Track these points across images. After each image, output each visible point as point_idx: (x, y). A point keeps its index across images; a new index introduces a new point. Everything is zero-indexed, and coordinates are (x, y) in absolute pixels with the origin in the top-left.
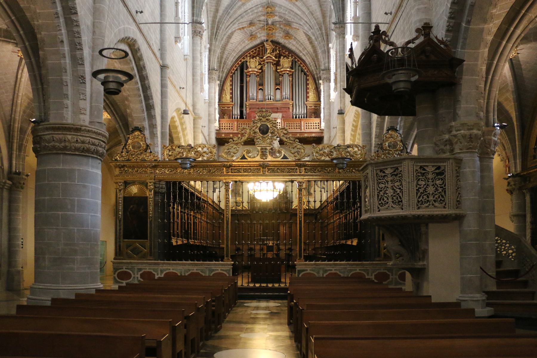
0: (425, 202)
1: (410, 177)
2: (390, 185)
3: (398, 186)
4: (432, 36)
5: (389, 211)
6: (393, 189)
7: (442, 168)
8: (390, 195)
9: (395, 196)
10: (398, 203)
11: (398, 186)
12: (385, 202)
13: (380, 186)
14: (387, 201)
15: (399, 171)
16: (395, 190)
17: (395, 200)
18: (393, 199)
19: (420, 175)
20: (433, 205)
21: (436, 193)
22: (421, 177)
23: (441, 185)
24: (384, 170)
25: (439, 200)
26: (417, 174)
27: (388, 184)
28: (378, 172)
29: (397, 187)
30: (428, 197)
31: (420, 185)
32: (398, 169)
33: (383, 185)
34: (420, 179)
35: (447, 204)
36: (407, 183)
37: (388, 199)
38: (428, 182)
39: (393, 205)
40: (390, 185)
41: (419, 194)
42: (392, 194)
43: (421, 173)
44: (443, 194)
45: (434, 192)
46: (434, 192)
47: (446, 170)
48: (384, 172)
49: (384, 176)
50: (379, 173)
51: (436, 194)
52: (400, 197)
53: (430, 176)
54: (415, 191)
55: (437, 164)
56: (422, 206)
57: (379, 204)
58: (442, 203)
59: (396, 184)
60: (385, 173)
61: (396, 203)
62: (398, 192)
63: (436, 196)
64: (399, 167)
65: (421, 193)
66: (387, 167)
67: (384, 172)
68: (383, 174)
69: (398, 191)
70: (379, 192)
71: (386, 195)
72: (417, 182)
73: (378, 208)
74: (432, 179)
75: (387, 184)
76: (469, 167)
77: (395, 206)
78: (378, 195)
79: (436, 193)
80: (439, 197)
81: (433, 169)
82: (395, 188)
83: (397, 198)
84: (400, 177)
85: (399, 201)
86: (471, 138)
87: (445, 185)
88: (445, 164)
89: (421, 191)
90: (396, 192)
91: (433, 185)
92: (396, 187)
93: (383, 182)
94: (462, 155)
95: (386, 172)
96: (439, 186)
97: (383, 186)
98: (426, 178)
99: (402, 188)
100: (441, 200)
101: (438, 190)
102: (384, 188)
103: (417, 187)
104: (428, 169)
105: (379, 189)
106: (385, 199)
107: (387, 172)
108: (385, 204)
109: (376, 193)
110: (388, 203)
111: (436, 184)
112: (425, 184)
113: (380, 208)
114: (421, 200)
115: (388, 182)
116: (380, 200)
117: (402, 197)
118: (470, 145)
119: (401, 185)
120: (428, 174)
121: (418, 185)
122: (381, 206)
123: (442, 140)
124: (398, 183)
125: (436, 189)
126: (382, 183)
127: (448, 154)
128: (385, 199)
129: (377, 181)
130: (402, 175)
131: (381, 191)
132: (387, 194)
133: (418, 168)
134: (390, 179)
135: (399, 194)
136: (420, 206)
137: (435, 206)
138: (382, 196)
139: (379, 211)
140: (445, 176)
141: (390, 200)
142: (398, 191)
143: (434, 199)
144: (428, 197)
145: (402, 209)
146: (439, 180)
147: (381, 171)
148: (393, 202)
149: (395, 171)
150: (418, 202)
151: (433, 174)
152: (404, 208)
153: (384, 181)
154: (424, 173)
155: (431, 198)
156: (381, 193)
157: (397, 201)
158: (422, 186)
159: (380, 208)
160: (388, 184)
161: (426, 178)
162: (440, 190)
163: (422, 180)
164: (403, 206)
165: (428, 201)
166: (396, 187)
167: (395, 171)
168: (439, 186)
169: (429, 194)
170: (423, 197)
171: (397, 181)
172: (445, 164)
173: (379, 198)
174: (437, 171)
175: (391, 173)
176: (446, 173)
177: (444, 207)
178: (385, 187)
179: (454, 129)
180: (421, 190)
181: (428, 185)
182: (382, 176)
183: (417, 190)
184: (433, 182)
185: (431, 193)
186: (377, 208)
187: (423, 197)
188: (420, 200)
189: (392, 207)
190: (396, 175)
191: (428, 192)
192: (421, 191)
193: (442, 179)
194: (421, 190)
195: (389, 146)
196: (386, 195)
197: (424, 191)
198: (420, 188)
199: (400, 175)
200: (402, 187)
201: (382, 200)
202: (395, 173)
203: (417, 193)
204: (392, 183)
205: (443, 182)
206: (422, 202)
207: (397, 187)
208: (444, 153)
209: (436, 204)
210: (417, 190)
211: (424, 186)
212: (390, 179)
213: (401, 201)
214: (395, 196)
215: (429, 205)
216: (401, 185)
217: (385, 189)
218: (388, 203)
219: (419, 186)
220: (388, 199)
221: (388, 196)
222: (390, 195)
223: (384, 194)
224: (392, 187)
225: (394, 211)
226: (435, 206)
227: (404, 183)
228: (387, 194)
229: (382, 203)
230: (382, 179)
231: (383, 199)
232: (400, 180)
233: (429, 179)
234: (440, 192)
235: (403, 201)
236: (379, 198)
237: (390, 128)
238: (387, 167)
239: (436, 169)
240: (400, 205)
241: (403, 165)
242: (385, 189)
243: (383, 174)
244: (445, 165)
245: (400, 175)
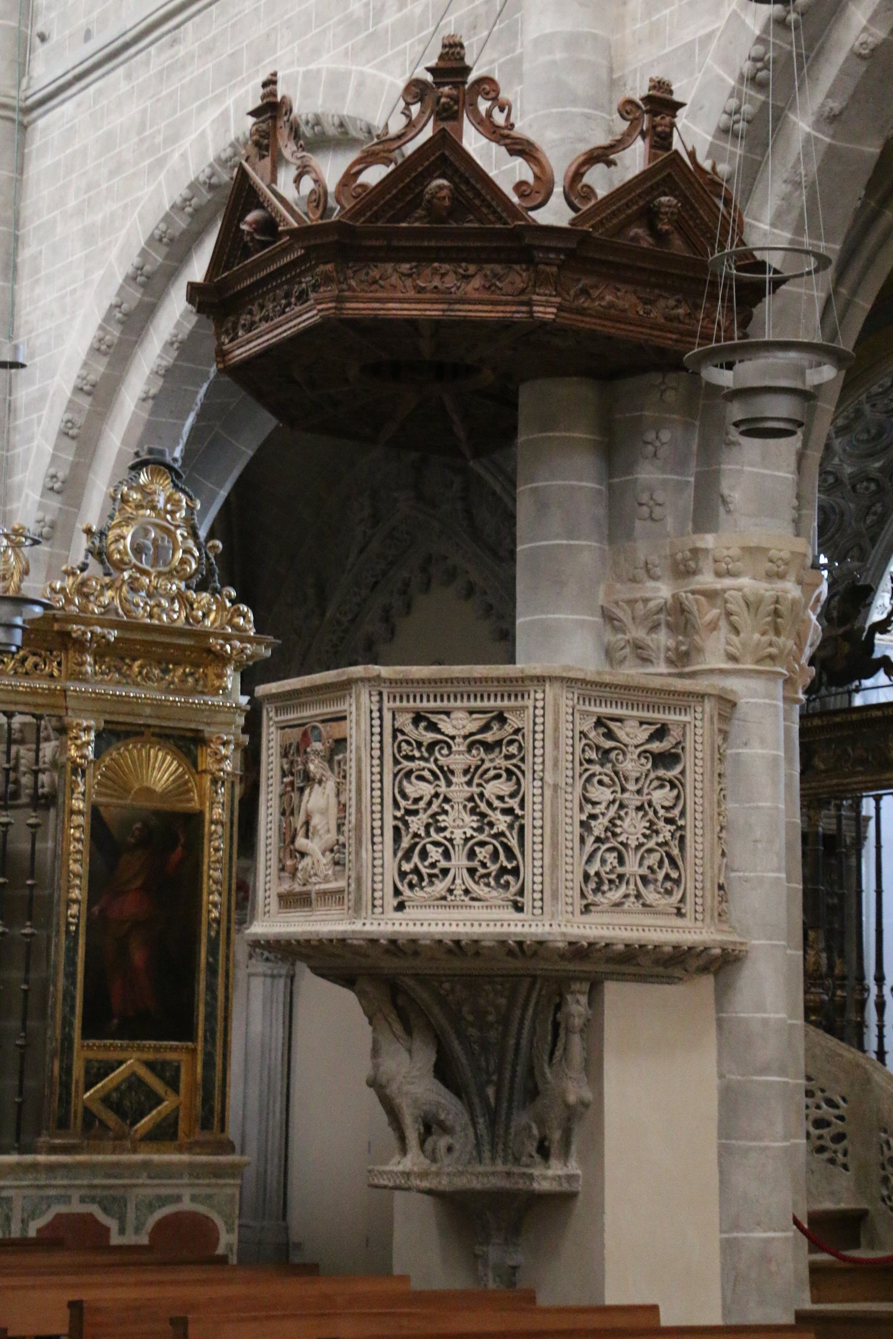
0: (611, 881)
1: (563, 764)
2: (459, 790)
3: (501, 798)
4: (676, 145)
5: (456, 914)
6: (473, 811)
7: (675, 735)
8: (458, 836)
9: (482, 844)
10: (497, 878)
11: (501, 798)
12: (433, 865)
13: (409, 789)
14: (443, 864)
15: (509, 729)
16: (483, 815)
17: (484, 865)
18: (472, 855)
19: (594, 756)
20: (638, 896)
21: (651, 844)
22: (596, 768)
23: (667, 809)
24: (434, 718)
25: (661, 875)
26: (583, 751)
27: (449, 783)
28: (405, 721)
29: (497, 803)
30: (621, 860)
31: (594, 804)
32: (501, 718)
33: (423, 785)
34: (593, 775)
35: (689, 899)
36: (548, 793)
37: (447, 855)
38: (624, 790)
40: (459, 790)
41: (589, 846)
42: (470, 832)
43: (598, 748)
44: (675, 852)
45: (642, 840)
46: (642, 840)
47: (689, 745)
48: (433, 727)
49: (431, 747)
50: (409, 728)
51: (650, 851)
52: (508, 850)
53: (631, 765)
54: (578, 830)
55: (656, 715)
56: (599, 898)
57: (403, 875)
58: (669, 892)
59: (492, 789)
60: (438, 731)
61: (488, 875)
62: (502, 827)
63: (652, 860)
64: (512, 709)
65: (598, 840)
66: (452, 704)
67: (433, 727)
68: (430, 737)
69: (502, 822)
70: (402, 819)
71: (436, 837)
72: (585, 788)
73: (397, 892)
74: (637, 780)
75: (442, 782)
76: (763, 742)
77: (479, 890)
78: (396, 829)
79: (651, 844)
80: (661, 863)
81: (643, 734)
82: (483, 807)
83: (495, 856)
84: (508, 757)
85: (503, 871)
86: (776, 613)
87: (683, 814)
88: (687, 718)
89: (596, 832)
90: (491, 825)
91: (639, 808)
92: (489, 804)
93: (426, 774)
94: (734, 684)
95: (441, 725)
96: (662, 812)
97: (426, 790)
98: (616, 773)
99: (518, 811)
100: (667, 877)
101: (657, 832)
102: (430, 803)
103: (582, 809)
104: (621, 734)
105: (403, 803)
106: (435, 854)
107: (446, 726)
108: (431, 876)
109: (389, 823)
110: (445, 872)
111: (650, 804)
112: (613, 802)
113: (406, 892)
114: (597, 874)
115: (447, 773)
116: (408, 856)
117: (517, 851)
118: (771, 645)
119: (512, 795)
120: (624, 754)
121: (588, 800)
122: (411, 886)
123: (640, 605)
124: (503, 787)
125: (652, 823)
126: (421, 778)
127: (663, 668)
128: (435, 854)
129: (396, 762)
130: (520, 748)
131: (415, 813)
133: (587, 725)
134: (458, 760)
135: (502, 834)
136: (591, 898)
137: (644, 905)
138: (416, 835)
139: (401, 907)
140: (683, 772)
141: (459, 861)
142: (502, 822)
143: (644, 871)
144: (621, 860)
145: (519, 908)
146: (662, 786)
147: (418, 718)
148: (472, 871)
149: (486, 728)
150: (586, 877)
151: (639, 756)
152: (527, 900)
154: (607, 752)
155: (632, 867)
156: (416, 824)
157: (493, 868)
158: (601, 808)
159: (406, 892)
160: (449, 783)
161: (616, 773)
162: (666, 831)
163: (600, 782)
164: (521, 892)
165: (621, 877)
166: (489, 804)
167: (486, 728)
168: (662, 812)
169: (625, 845)
170: (603, 861)
171: (497, 777)
172: (687, 718)
173: (406, 843)
174: (656, 746)
175: (465, 737)
176: (688, 760)
177: (679, 913)
178: (437, 795)
179: (707, 566)
180: (598, 827)
181: (622, 806)
182: (419, 745)
183: (582, 823)
184: (639, 792)
185: (633, 843)
186: (390, 890)
187: (603, 861)
188: (592, 872)
189: (467, 892)
190: (489, 747)
191: (622, 838)
192: (596, 832)
193: (673, 786)
194: (598, 827)
195: (138, 550)
196: (436, 837)
197: (607, 829)
198: (593, 817)
199: (513, 749)
200: (522, 806)
201: (416, 859)
202: (489, 737)
203: (582, 840)
204: (469, 783)
205: (678, 797)
206: (600, 883)
207: (497, 803)
208: (646, 660)
209: (650, 895)
210: (582, 823)
211: (607, 808)
212: (458, 760)
213: (515, 872)
214: (482, 844)
215: (626, 896)
216: (512, 795)
217: (435, 808)
218: (445, 872)
219: (589, 808)
220: (447, 855)
221: (451, 840)
222: (458, 836)
223: (427, 826)
224: (471, 799)
225: (477, 912)
226: (644, 905)
227: (529, 786)
228: (444, 829)
229: (416, 871)
230: (422, 758)
231: (424, 855)
232: (510, 773)
233: (626, 779)
234: (666, 843)
235: (527, 873)
236: (406, 843)
237: (144, 456)
238: (452, 704)
239: (652, 738)
240: (507, 885)
241: (530, 703)
242: (435, 808)
243: (430, 737)
244: (684, 725)
245: (513, 749)
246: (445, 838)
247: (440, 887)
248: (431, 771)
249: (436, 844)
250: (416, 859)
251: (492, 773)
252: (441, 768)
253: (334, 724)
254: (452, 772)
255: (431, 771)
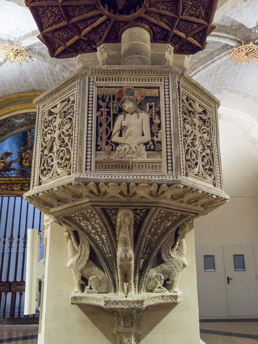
9: (204, 156)
18: (203, 160)
28: (184, 98)
39: (203, 172)
68: (190, 109)
69: (208, 151)
106: (194, 155)
126: (188, 123)
131: (186, 136)
132: (194, 146)
148: (203, 166)
153: (191, 120)
173: (186, 148)
175: (199, 113)
178: (192, 132)
221: (197, 151)
224: (200, 137)
231: (191, 154)
246: (196, 149)
247: (196, 170)
248: (190, 121)
249: (194, 152)
250: (189, 156)
251: (204, 131)
252: (193, 121)
253: (148, 90)
254: (195, 125)
255: (190, 121)
